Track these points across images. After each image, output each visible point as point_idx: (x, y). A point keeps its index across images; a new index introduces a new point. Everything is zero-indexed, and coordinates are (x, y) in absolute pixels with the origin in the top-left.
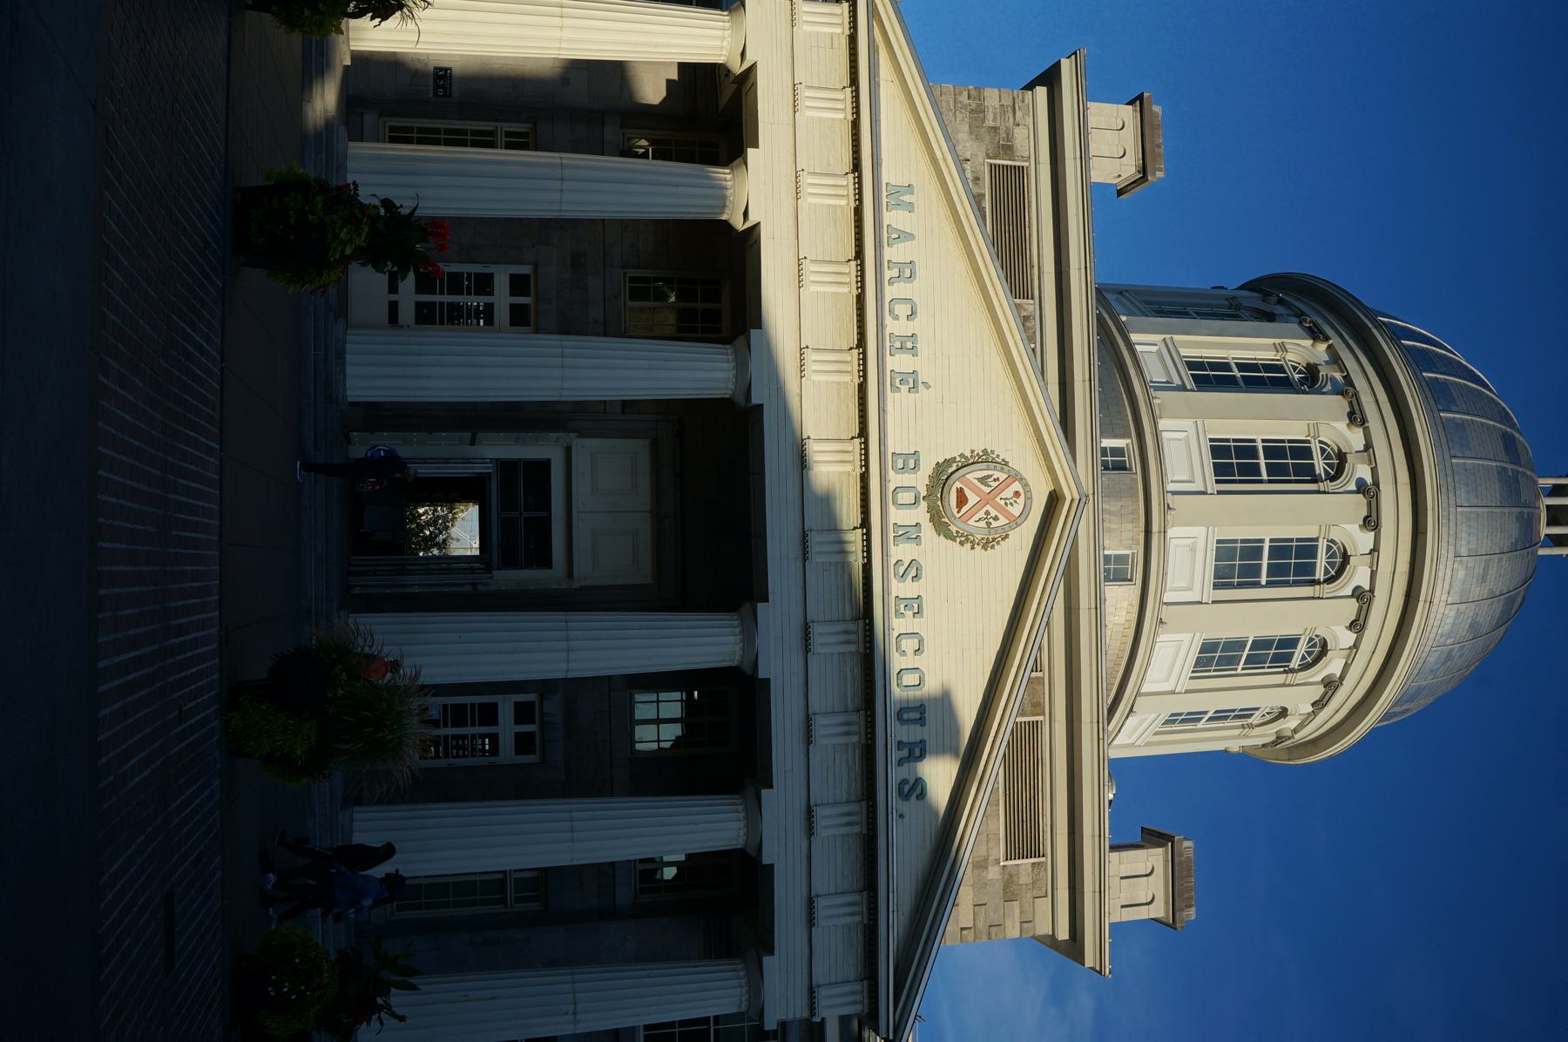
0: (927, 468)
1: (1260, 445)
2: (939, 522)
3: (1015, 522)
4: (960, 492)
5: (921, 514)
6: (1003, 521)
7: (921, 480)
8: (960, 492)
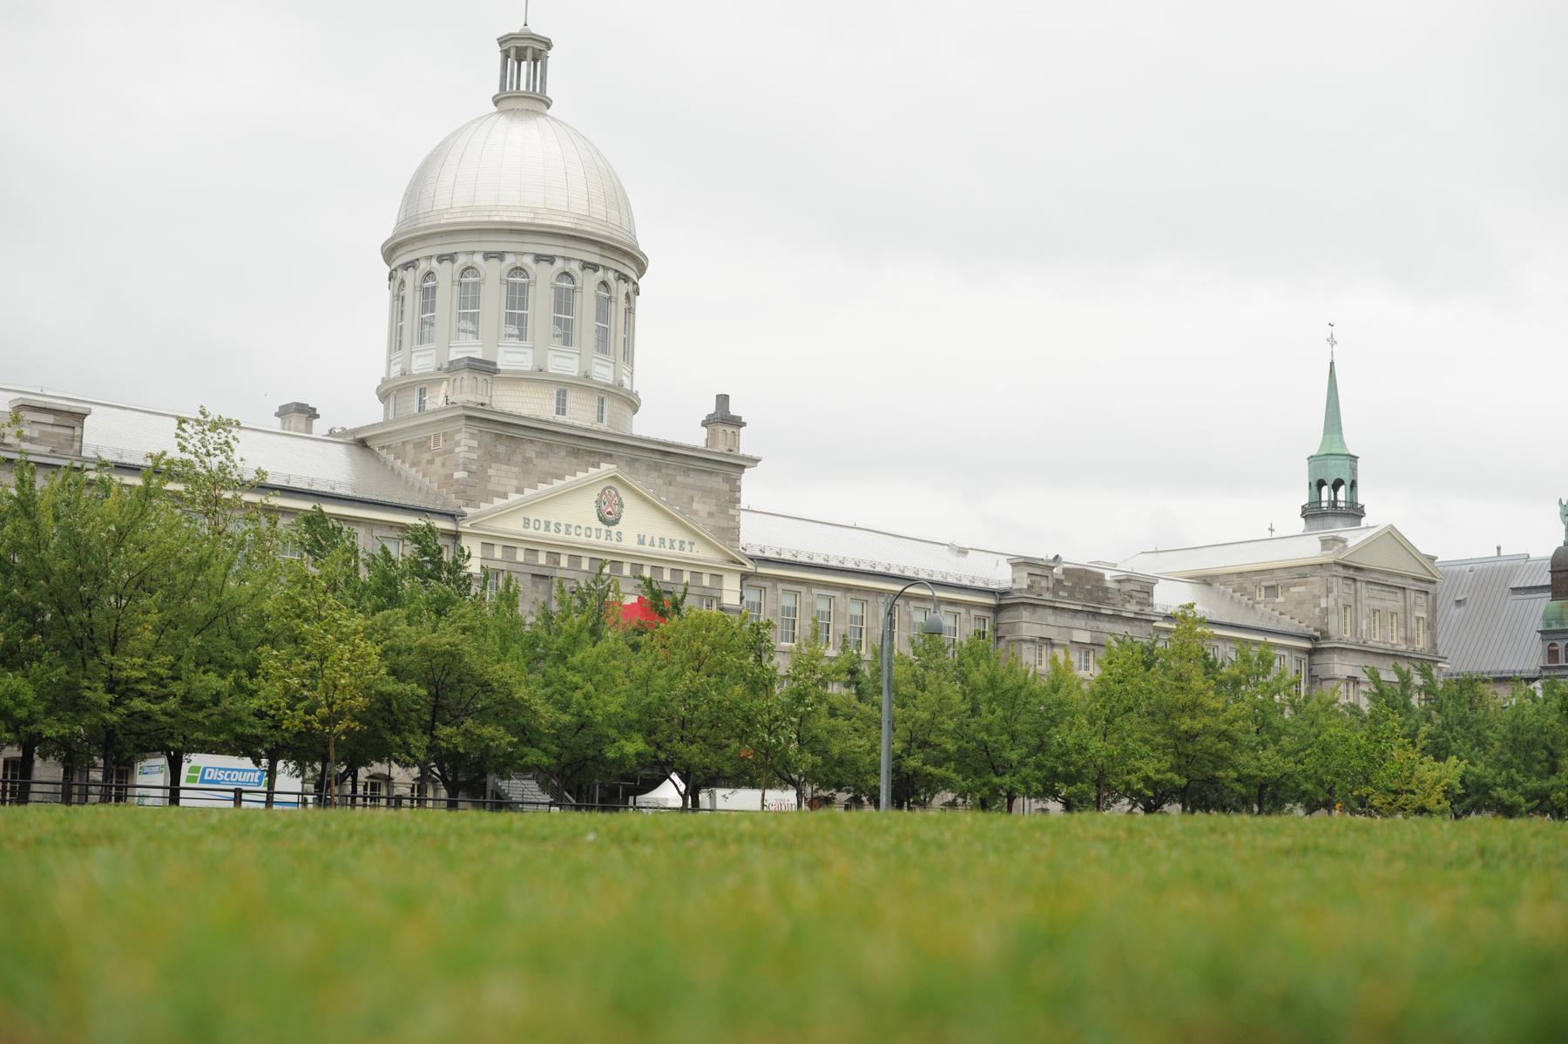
0: (600, 525)
1: (525, 312)
3: (617, 494)
5: (614, 529)
6: (616, 499)
7: (604, 527)
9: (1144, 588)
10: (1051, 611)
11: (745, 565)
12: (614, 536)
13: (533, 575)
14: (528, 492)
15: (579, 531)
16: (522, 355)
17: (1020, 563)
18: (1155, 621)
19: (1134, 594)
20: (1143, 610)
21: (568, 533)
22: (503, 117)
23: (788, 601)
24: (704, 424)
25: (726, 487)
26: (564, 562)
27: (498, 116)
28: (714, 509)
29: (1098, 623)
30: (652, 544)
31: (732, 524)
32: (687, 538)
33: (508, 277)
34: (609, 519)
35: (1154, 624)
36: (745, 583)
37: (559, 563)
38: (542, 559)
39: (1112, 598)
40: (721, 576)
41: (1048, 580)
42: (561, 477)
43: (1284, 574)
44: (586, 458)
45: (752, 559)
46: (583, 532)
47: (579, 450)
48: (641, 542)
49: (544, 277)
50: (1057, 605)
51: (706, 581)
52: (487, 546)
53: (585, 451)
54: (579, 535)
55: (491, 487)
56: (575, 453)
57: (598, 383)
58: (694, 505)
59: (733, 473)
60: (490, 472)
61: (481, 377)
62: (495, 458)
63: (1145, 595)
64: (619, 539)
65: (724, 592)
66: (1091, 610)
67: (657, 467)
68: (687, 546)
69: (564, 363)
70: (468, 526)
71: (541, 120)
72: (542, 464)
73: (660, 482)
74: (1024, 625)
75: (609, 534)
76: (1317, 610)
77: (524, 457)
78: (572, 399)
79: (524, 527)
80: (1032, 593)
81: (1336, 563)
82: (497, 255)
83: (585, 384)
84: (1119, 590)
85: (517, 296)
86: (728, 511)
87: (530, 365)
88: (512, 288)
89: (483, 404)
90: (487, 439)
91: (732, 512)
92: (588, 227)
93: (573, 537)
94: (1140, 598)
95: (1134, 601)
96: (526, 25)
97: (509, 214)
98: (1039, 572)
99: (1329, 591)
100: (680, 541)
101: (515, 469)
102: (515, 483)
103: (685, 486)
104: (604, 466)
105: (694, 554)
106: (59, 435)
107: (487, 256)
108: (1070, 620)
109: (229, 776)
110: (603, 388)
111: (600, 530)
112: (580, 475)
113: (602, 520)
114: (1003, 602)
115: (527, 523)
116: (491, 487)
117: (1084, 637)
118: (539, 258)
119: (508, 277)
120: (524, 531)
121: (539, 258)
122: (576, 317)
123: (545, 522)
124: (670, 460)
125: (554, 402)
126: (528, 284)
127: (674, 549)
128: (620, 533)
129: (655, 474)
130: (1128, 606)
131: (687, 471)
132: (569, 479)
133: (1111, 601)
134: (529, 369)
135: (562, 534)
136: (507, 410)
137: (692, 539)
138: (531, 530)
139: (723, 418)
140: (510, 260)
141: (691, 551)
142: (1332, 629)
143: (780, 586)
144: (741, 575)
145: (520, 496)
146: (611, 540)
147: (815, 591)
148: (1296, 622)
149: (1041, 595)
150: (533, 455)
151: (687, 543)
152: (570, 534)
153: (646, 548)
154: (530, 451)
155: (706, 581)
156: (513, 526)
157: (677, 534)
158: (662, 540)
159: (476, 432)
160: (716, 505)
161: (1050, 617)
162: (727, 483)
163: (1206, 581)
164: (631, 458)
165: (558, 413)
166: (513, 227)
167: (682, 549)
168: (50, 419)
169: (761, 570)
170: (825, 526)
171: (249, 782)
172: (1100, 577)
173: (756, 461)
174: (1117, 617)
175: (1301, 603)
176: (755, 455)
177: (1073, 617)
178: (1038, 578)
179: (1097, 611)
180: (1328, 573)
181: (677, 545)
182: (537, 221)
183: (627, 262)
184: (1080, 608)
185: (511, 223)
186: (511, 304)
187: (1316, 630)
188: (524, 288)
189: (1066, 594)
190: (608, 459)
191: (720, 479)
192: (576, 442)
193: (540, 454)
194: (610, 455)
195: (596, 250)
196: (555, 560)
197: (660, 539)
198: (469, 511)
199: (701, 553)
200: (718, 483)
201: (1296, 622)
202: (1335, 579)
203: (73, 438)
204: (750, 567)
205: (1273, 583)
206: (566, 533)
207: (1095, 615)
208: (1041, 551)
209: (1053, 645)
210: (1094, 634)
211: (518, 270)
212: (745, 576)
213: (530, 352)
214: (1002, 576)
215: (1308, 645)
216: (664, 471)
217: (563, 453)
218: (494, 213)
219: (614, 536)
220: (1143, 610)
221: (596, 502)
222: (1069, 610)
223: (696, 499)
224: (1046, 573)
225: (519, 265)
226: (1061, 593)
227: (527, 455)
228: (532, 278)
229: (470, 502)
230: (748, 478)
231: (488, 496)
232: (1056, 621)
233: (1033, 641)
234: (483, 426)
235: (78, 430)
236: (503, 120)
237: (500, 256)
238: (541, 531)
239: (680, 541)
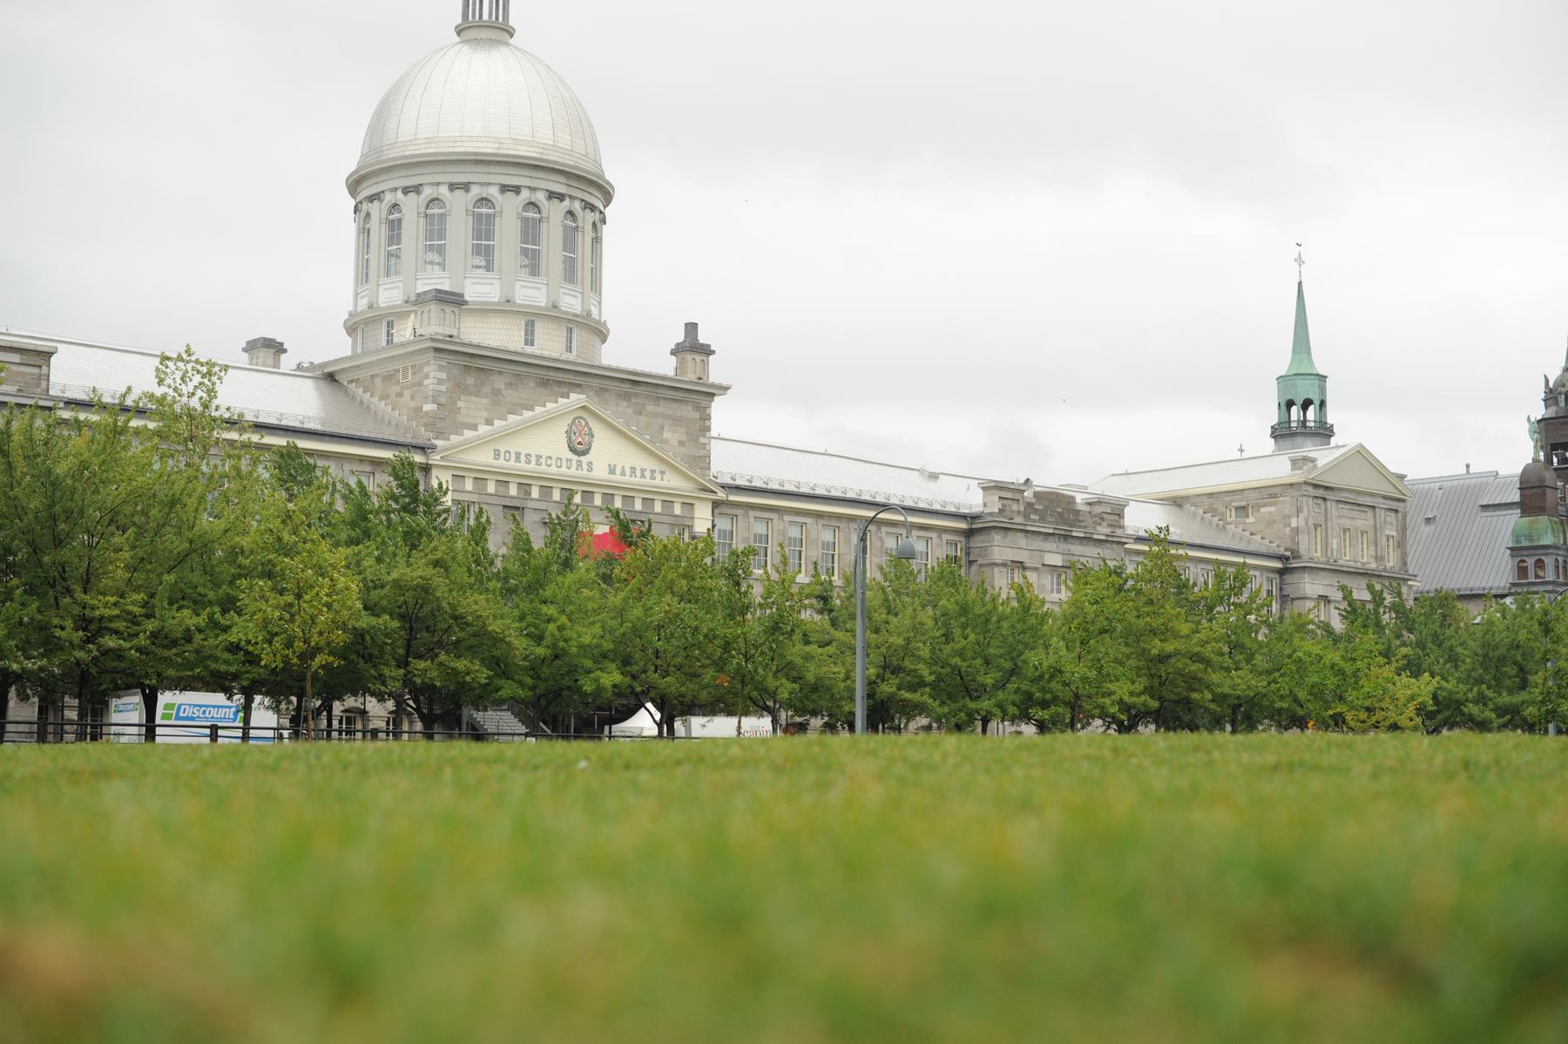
0: (571, 455)
1: (491, 243)
2: (585, 453)
3: (587, 424)
4: (578, 443)
5: (585, 459)
7: (575, 458)
8: (578, 443)
9: (1116, 511)
10: (1022, 535)
11: (716, 493)
12: (585, 467)
13: (504, 506)
14: (498, 423)
15: (549, 462)
16: (489, 287)
17: (991, 487)
18: (1126, 543)
19: (1105, 516)
20: (1114, 532)
23: (760, 528)
24: (673, 353)
25: (696, 415)
26: (535, 493)
27: (461, 45)
28: (684, 438)
30: (623, 473)
31: (702, 452)
32: (658, 467)
33: (474, 208)
34: (580, 449)
35: (1126, 546)
36: (716, 511)
37: (530, 494)
38: (513, 491)
39: (1082, 521)
40: (692, 504)
41: (1019, 504)
42: (531, 408)
43: (1254, 495)
45: (723, 487)
46: (554, 462)
47: (548, 380)
48: (612, 471)
49: (509, 209)
50: (1028, 528)
51: (678, 510)
53: (554, 381)
54: (549, 466)
55: (460, 418)
56: (545, 383)
57: (566, 313)
58: (664, 433)
59: (703, 401)
60: (460, 404)
61: (448, 309)
62: (465, 390)
63: (1117, 518)
64: (590, 469)
65: (696, 520)
66: (1062, 532)
67: (626, 396)
68: (658, 475)
69: (532, 294)
70: (438, 457)
71: (504, 49)
72: (511, 396)
73: (630, 411)
74: (996, 549)
75: (579, 464)
76: (1288, 530)
78: (540, 329)
79: (495, 458)
80: (1004, 517)
81: (1305, 483)
82: (462, 186)
83: (553, 315)
84: (1090, 513)
85: (483, 227)
86: (698, 439)
87: (498, 297)
88: (478, 218)
89: (451, 336)
90: (455, 371)
91: (702, 440)
92: (554, 157)
93: (544, 467)
94: (1111, 520)
95: (1104, 524)
97: (474, 144)
98: (1009, 495)
99: (1299, 511)
100: (651, 470)
101: (484, 401)
102: (485, 414)
103: (655, 415)
104: (573, 396)
105: (665, 483)
106: (26, 374)
107: (453, 187)
108: (1042, 543)
109: (204, 712)
110: (571, 318)
111: (571, 460)
112: (550, 406)
113: (573, 450)
114: (974, 526)
115: (497, 454)
116: (460, 418)
117: (1056, 560)
118: (504, 189)
119: (474, 208)
120: (496, 463)
121: (504, 189)
122: (543, 248)
123: (516, 453)
124: (639, 389)
125: (523, 333)
126: (494, 215)
127: (645, 478)
128: (591, 463)
129: (625, 404)
130: (1099, 528)
131: (657, 399)
132: (538, 409)
133: (1082, 524)
134: (496, 300)
135: (533, 465)
136: (475, 341)
137: (663, 468)
138: (501, 462)
139: (692, 347)
140: (476, 191)
141: (662, 480)
142: (1303, 549)
143: (752, 513)
144: (713, 503)
145: (489, 428)
146: (582, 470)
147: (787, 518)
148: (1266, 542)
149: (1012, 519)
150: (502, 386)
151: (658, 472)
152: (541, 465)
153: (617, 477)
154: (499, 382)
155: (678, 510)
156: (483, 458)
157: (648, 464)
158: (633, 470)
159: (445, 364)
160: (687, 434)
161: (1022, 541)
162: (697, 411)
163: (1176, 502)
164: (600, 388)
165: (526, 344)
166: (478, 158)
167: (653, 478)
168: (16, 358)
169: (732, 498)
170: (795, 452)
171: (224, 718)
172: (1071, 500)
173: (726, 389)
174: (1087, 540)
175: (1271, 523)
176: (725, 383)
177: (1045, 540)
178: (1009, 502)
179: (1069, 533)
180: (1298, 493)
181: (648, 474)
182: (502, 152)
183: (592, 190)
184: (1051, 531)
185: (476, 154)
186: (478, 234)
187: (1286, 550)
188: (490, 219)
189: (1037, 518)
190: (578, 390)
191: (690, 408)
193: (510, 385)
194: (579, 386)
195: (562, 179)
196: (526, 491)
197: (631, 468)
198: (439, 443)
199: (671, 482)
200: (688, 412)
201: (1266, 542)
202: (1305, 499)
203: (40, 377)
204: (721, 495)
205: (1243, 503)
206: (536, 464)
207: (1067, 537)
208: (1011, 475)
209: (1024, 568)
210: (1066, 557)
211: (484, 201)
212: (716, 504)
213: (497, 283)
214: (973, 500)
215: (1279, 565)
216: (634, 400)
217: (532, 384)
218: (458, 144)
219: (585, 467)
220: (1114, 532)
221: (566, 432)
222: (1040, 533)
223: (666, 427)
224: (1017, 496)
225: (484, 196)
226: (1032, 517)
228: (498, 208)
229: (440, 434)
230: (718, 407)
231: (459, 428)
233: (1005, 565)
234: (452, 358)
235: (44, 368)
236: (466, 49)
237: (466, 187)
238: (512, 463)
239: (651, 470)
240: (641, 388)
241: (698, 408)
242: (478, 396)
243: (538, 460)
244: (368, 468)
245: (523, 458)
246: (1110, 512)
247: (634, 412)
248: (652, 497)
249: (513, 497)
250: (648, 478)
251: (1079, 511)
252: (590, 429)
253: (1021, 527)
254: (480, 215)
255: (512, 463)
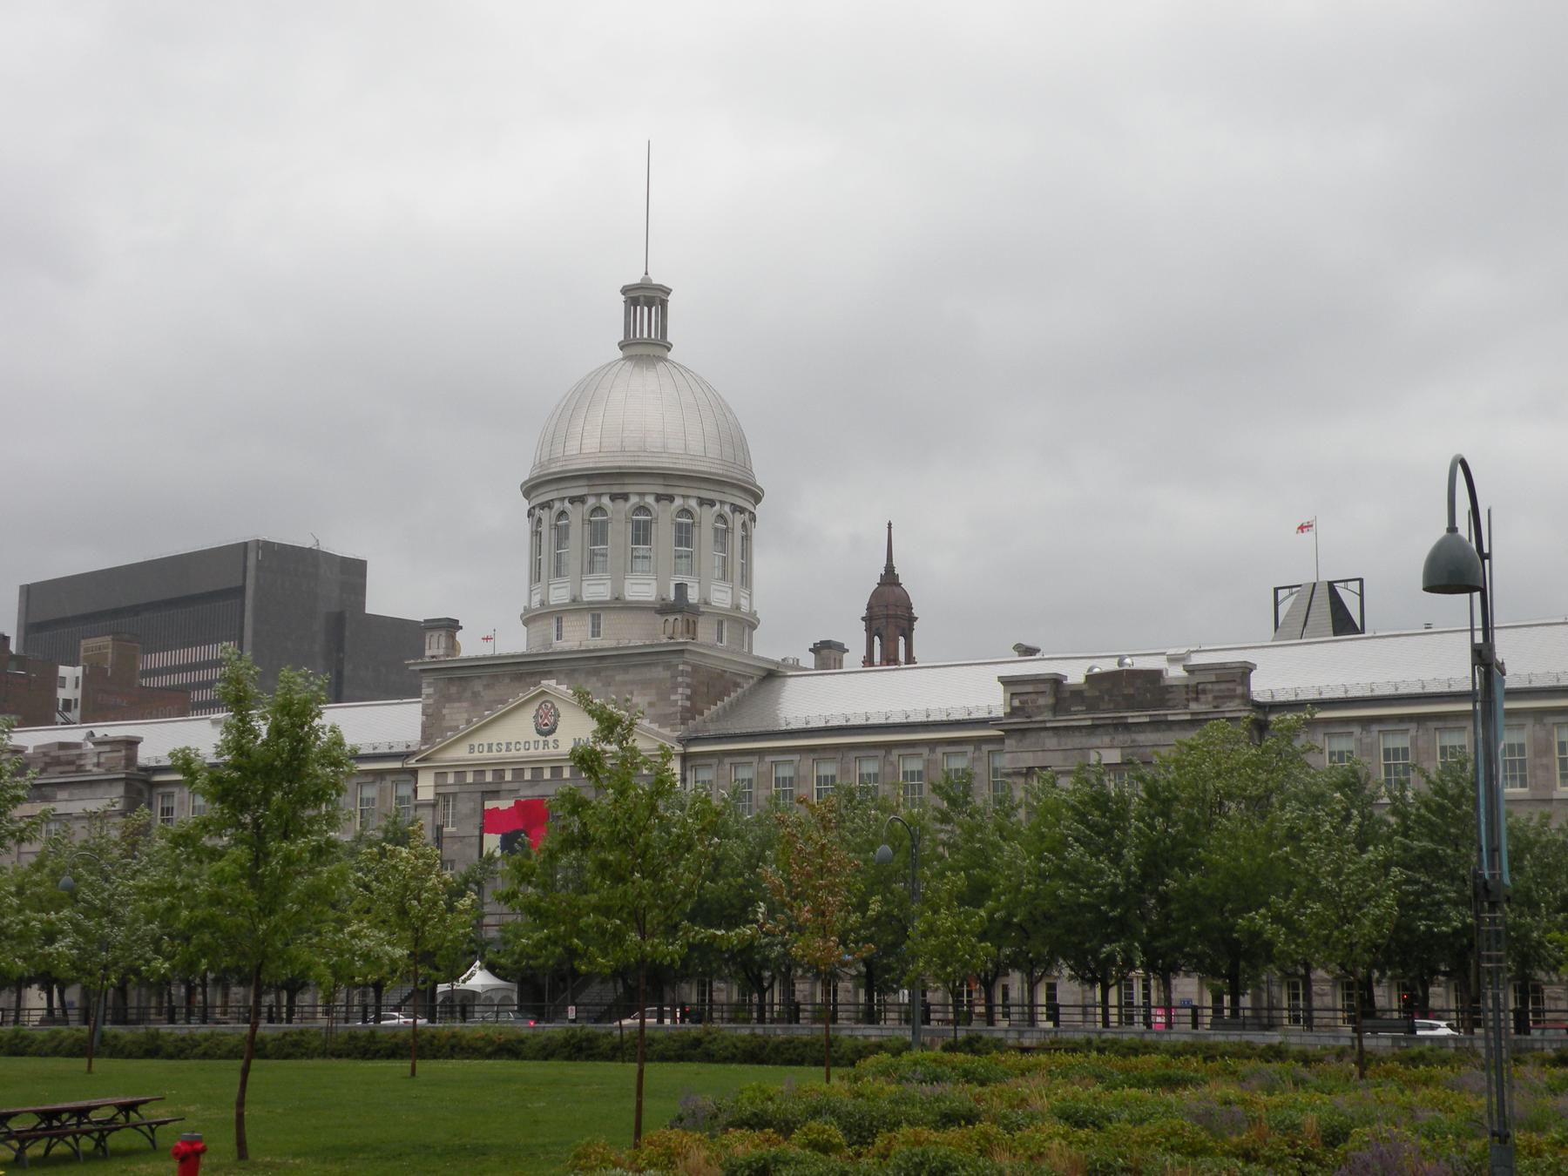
3: (553, 706)
5: (550, 738)
10: (1050, 733)
12: (551, 744)
19: (1209, 686)
21: (508, 749)
22: (628, 363)
25: (668, 674)
26: (508, 776)
29: (1134, 736)
36: (689, 765)
38: (489, 778)
44: (528, 680)
46: (522, 746)
52: (441, 775)
55: (446, 724)
60: (445, 711)
66: (1109, 721)
67: (596, 672)
70: (414, 761)
72: (488, 695)
73: (600, 685)
75: (546, 744)
77: (473, 693)
83: (577, 606)
94: (1220, 690)
95: (1210, 697)
96: (646, 274)
98: (1029, 688)
101: (465, 704)
113: (540, 732)
115: (472, 748)
116: (446, 724)
124: (605, 664)
129: (595, 679)
131: (626, 669)
135: (532, 750)
138: (476, 754)
150: (481, 689)
154: (478, 686)
156: (461, 753)
161: (1051, 742)
168: (107, 748)
170: (981, 667)
178: (1033, 696)
179: (1125, 721)
191: (660, 669)
192: (515, 668)
193: (487, 686)
207: (1127, 727)
217: (507, 681)
219: (551, 744)
223: (635, 693)
227: (476, 690)
232: (1059, 744)
240: (609, 661)
241: (668, 666)
242: (459, 702)
243: (507, 747)
244: (370, 779)
245: (494, 747)
246: (1214, 679)
247: (603, 685)
248: (501, 767)
249: (490, 783)
250: (504, 750)
251: (1172, 686)
252: (556, 710)
253: (1042, 725)
254: (596, 522)
255: (485, 754)
